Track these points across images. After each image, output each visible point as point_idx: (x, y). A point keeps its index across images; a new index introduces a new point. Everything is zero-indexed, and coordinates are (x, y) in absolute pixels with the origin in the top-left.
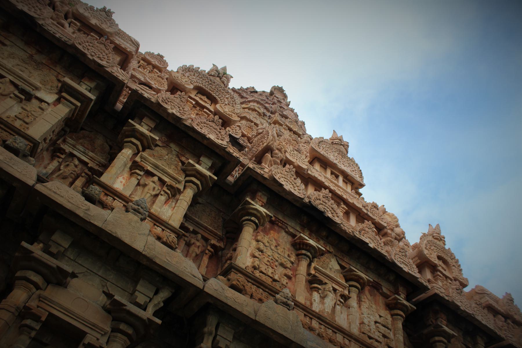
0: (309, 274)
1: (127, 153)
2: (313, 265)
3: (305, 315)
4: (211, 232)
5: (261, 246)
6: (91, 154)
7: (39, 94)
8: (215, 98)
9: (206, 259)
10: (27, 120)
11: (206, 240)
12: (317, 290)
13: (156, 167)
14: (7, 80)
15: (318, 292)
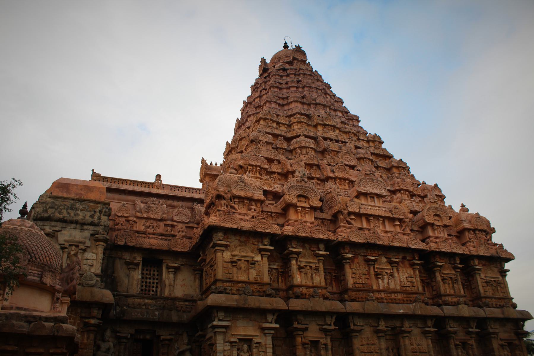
0: (375, 271)
1: (294, 262)
2: (376, 266)
3: (378, 293)
4: (331, 269)
5: (354, 271)
6: (277, 264)
7: (255, 259)
8: (307, 196)
9: (334, 283)
10: (260, 275)
11: (330, 273)
12: (380, 278)
13: (306, 262)
14: (243, 261)
15: (380, 279)
